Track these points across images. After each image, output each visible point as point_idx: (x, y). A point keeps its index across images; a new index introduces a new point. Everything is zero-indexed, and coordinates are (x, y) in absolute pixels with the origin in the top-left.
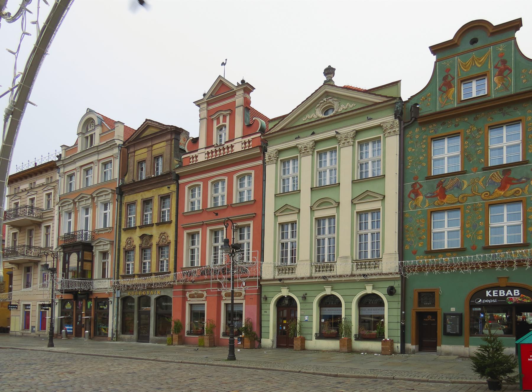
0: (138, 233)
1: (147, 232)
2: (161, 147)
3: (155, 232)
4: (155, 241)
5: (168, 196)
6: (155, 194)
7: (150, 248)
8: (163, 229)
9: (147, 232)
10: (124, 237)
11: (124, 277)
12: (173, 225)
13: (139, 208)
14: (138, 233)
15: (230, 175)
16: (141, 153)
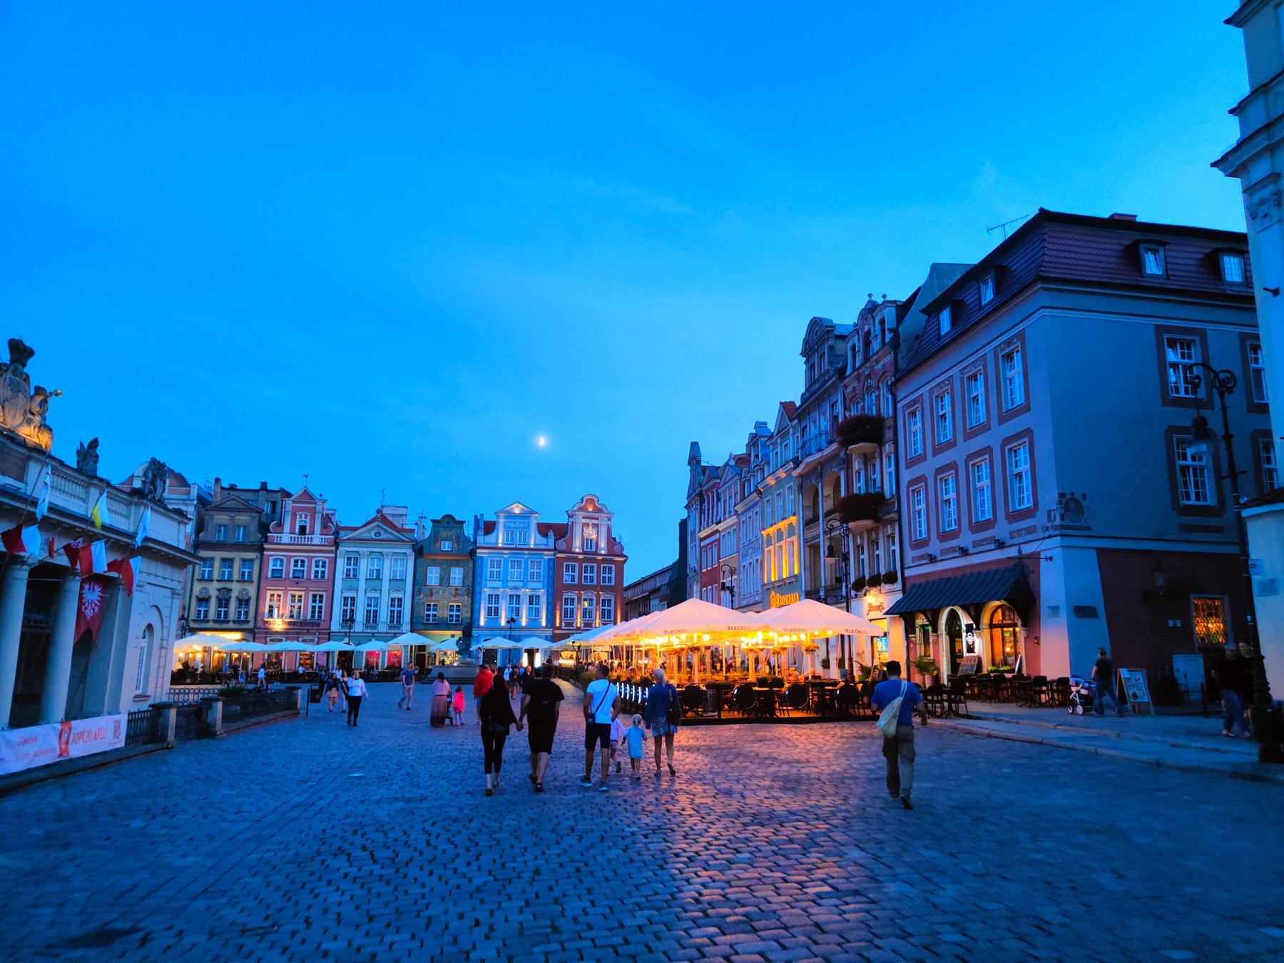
0: (216, 585)
1: (228, 585)
2: (242, 518)
3: (236, 588)
4: (234, 594)
5: (251, 561)
6: (237, 556)
7: (228, 601)
8: (246, 586)
9: (228, 585)
10: (197, 587)
11: (194, 621)
12: (255, 584)
13: (217, 564)
14: (216, 585)
15: (310, 558)
16: (222, 518)
